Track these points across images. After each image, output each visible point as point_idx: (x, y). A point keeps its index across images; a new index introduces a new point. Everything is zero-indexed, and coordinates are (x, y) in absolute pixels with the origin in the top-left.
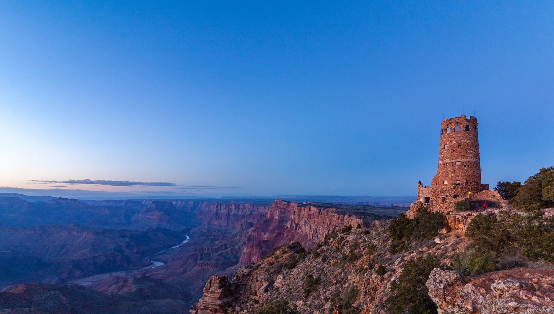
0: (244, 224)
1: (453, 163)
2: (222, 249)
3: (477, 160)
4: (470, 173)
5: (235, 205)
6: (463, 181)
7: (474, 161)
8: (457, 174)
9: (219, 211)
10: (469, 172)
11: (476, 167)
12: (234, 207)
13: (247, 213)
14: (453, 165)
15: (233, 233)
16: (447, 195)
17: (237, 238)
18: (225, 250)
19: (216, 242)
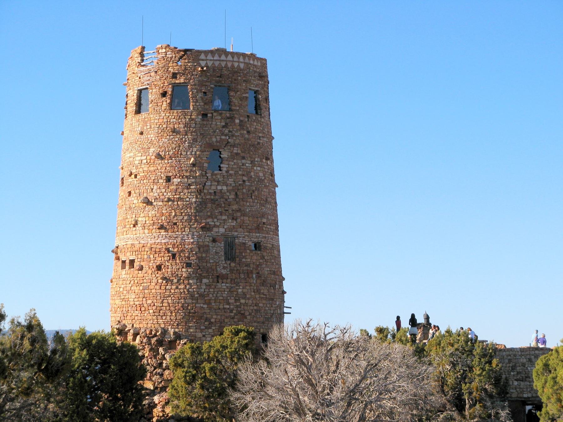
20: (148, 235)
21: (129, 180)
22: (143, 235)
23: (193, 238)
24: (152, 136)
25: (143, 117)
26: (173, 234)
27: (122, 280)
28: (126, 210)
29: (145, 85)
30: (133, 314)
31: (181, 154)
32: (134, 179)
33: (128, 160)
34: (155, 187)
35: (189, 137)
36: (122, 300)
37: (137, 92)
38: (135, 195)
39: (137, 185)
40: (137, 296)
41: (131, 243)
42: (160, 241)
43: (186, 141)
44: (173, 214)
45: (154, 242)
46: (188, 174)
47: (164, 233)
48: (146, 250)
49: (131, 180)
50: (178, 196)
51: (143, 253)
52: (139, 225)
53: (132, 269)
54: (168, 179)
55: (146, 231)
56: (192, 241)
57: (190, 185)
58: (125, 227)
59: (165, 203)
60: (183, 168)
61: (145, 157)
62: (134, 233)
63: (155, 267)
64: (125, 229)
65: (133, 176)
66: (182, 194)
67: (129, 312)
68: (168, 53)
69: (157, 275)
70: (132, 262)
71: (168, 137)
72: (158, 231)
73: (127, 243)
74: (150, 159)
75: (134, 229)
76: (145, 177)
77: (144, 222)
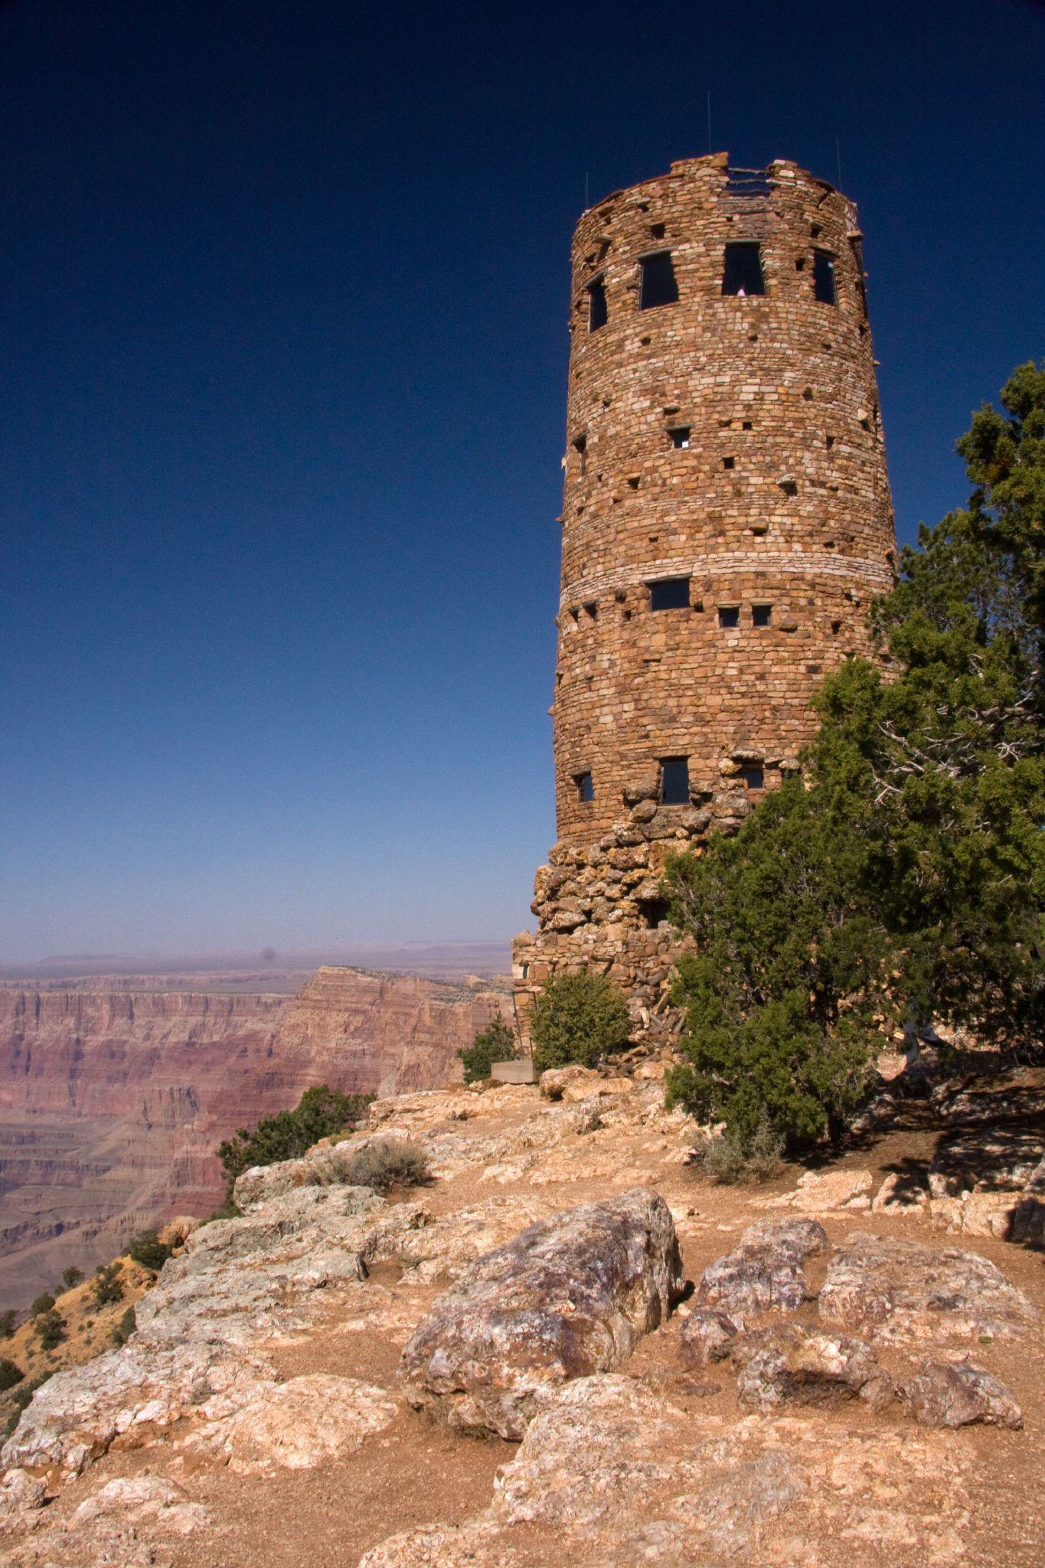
0: (156, 1095)
1: (621, 598)
2: (39, 1236)
3: (849, 566)
4: (781, 686)
5: (112, 1000)
6: (712, 763)
7: (810, 571)
8: (658, 700)
9: (30, 1034)
10: (761, 677)
11: (836, 626)
12: (106, 1007)
13: (173, 1039)
14: (628, 615)
15: (102, 1149)
16: (587, 904)
17: (120, 1173)
18: (57, 1241)
19: (7, 1195)
20: (803, 555)
21: (721, 434)
22: (791, 555)
23: (879, 575)
24: (785, 345)
25: (755, 303)
26: (851, 559)
27: (730, 650)
28: (721, 496)
29: (751, 236)
30: (783, 727)
31: (844, 397)
32: (745, 432)
33: (707, 391)
34: (807, 455)
35: (852, 365)
36: (739, 696)
37: (724, 247)
38: (752, 467)
39: (759, 445)
40: (795, 687)
41: (754, 569)
42: (831, 572)
43: (847, 372)
44: (848, 518)
45: (818, 571)
46: (859, 441)
47: (839, 556)
48: (804, 587)
49: (731, 434)
50: (851, 483)
51: (794, 593)
52: (773, 532)
53: (763, 628)
54: (830, 441)
55: (797, 547)
56: (879, 579)
57: (864, 463)
58: (722, 533)
59: (832, 493)
60: (852, 427)
61: (772, 389)
62: (758, 547)
63: (829, 625)
64: (720, 540)
65: (737, 425)
66: (855, 479)
67: (767, 721)
68: (799, 182)
69: (836, 644)
70: (761, 614)
71: (819, 355)
72: (825, 550)
73: (736, 569)
74: (787, 394)
75: (759, 539)
76: (777, 431)
77: (789, 527)
